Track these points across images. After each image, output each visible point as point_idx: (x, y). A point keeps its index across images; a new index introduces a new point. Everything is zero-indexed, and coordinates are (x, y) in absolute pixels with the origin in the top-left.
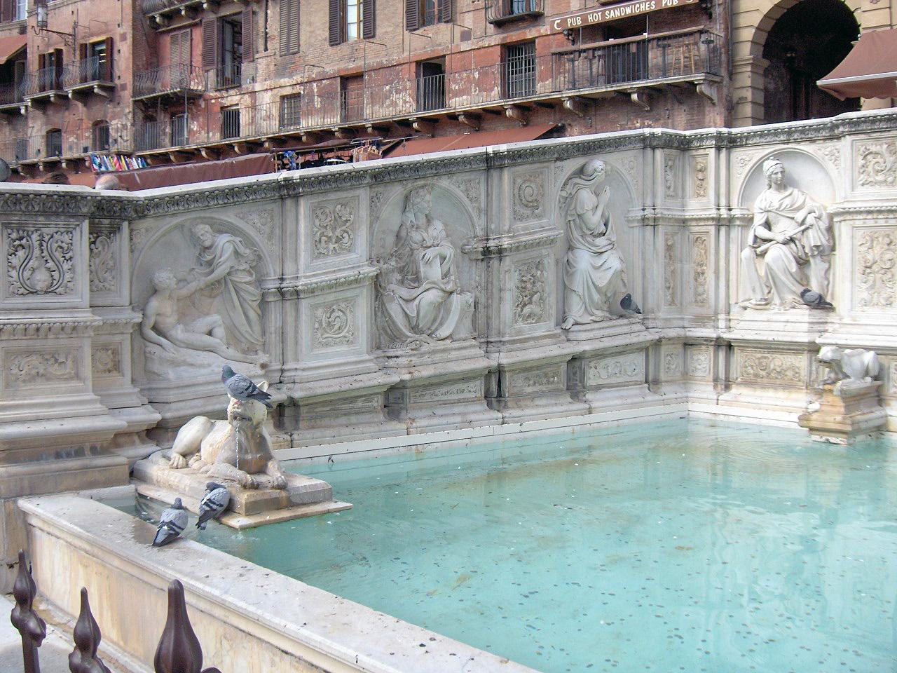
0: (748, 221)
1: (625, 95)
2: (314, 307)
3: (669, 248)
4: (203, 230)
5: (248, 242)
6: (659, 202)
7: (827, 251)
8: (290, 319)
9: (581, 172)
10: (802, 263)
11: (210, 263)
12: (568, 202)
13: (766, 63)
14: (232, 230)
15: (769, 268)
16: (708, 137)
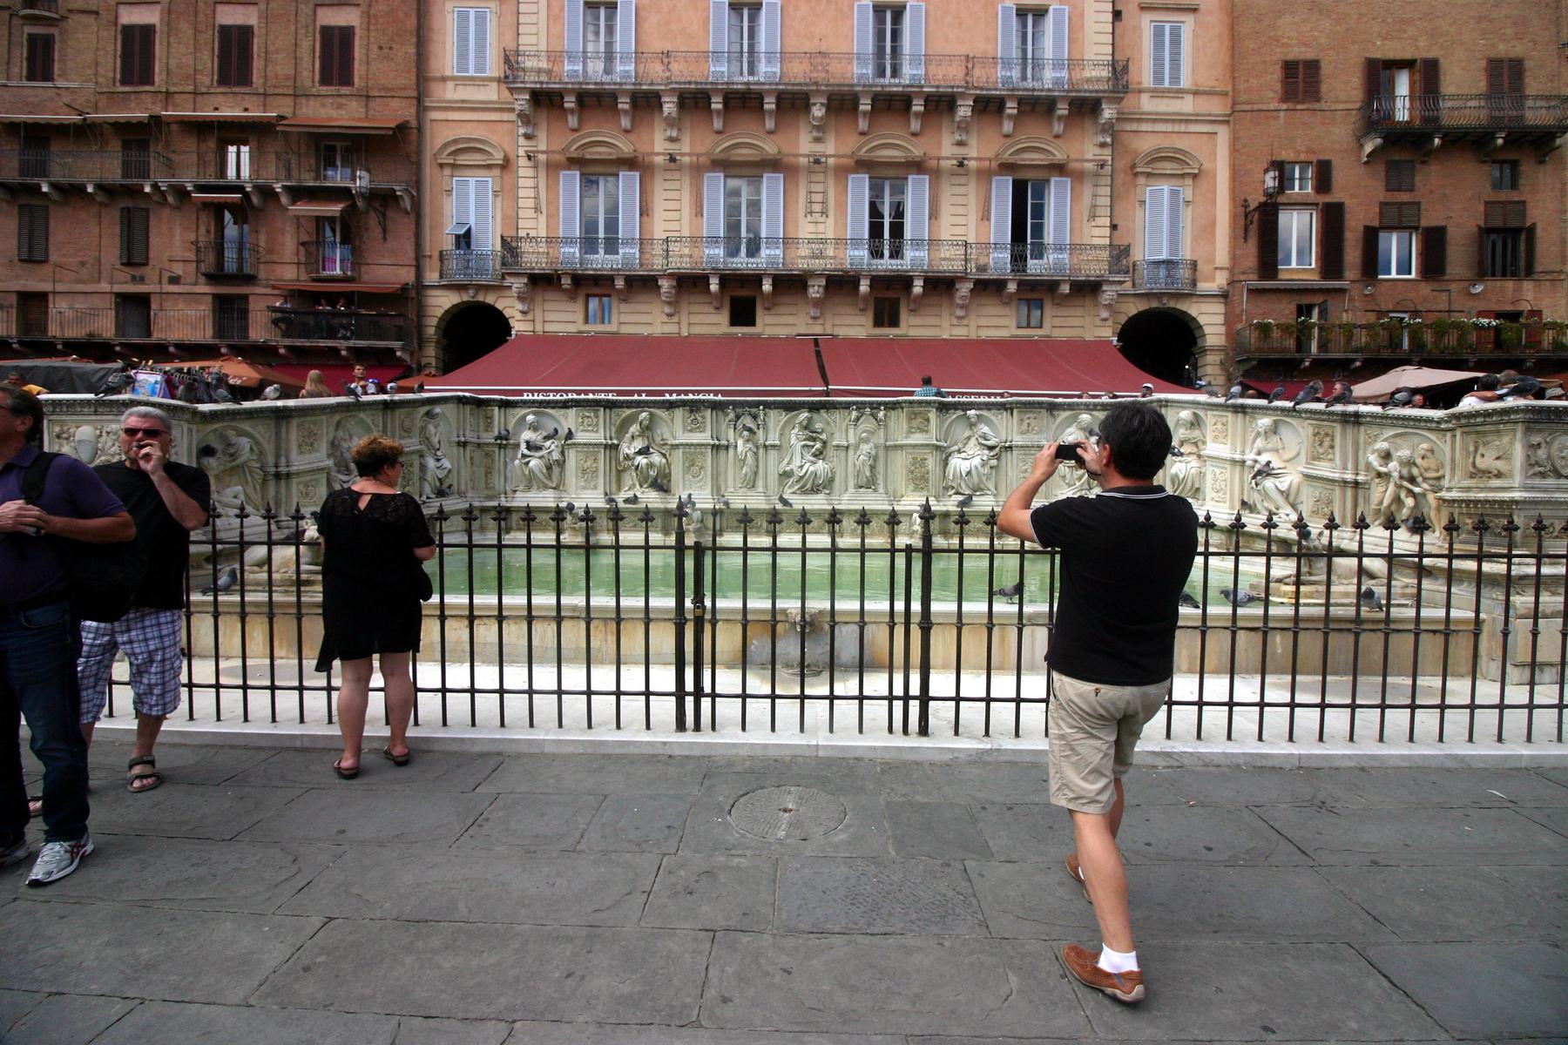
0: (517, 446)
1: (336, 351)
2: (299, 483)
3: (471, 458)
4: (231, 434)
5: (257, 443)
6: (467, 433)
7: (561, 464)
8: (283, 490)
9: (428, 414)
10: (549, 468)
11: (232, 455)
12: (423, 429)
13: (446, 342)
14: (247, 435)
15: (531, 471)
16: (494, 400)
